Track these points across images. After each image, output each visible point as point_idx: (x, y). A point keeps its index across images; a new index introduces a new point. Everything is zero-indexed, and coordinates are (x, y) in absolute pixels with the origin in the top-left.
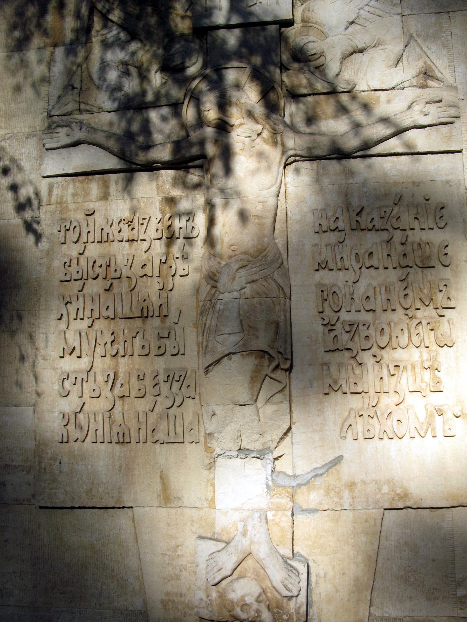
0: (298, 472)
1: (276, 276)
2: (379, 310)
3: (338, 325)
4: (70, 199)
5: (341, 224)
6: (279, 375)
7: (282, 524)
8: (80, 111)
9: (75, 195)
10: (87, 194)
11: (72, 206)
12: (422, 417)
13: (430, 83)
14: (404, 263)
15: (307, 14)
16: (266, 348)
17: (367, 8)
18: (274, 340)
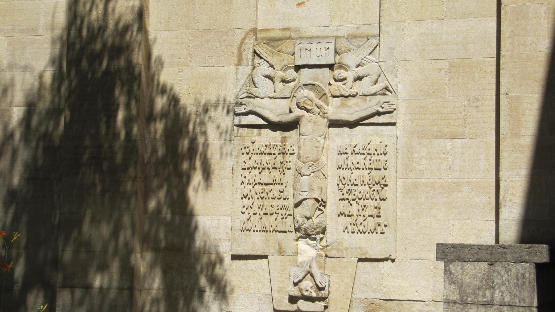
0: (328, 243)
1: (322, 170)
2: (359, 185)
3: (344, 190)
4: (246, 135)
5: (348, 151)
6: (321, 208)
7: (322, 262)
8: (250, 97)
9: (248, 133)
10: (253, 133)
11: (246, 138)
12: (373, 225)
13: (388, 93)
14: (370, 166)
15: (342, 61)
16: (317, 197)
17: (365, 59)
18: (320, 194)
